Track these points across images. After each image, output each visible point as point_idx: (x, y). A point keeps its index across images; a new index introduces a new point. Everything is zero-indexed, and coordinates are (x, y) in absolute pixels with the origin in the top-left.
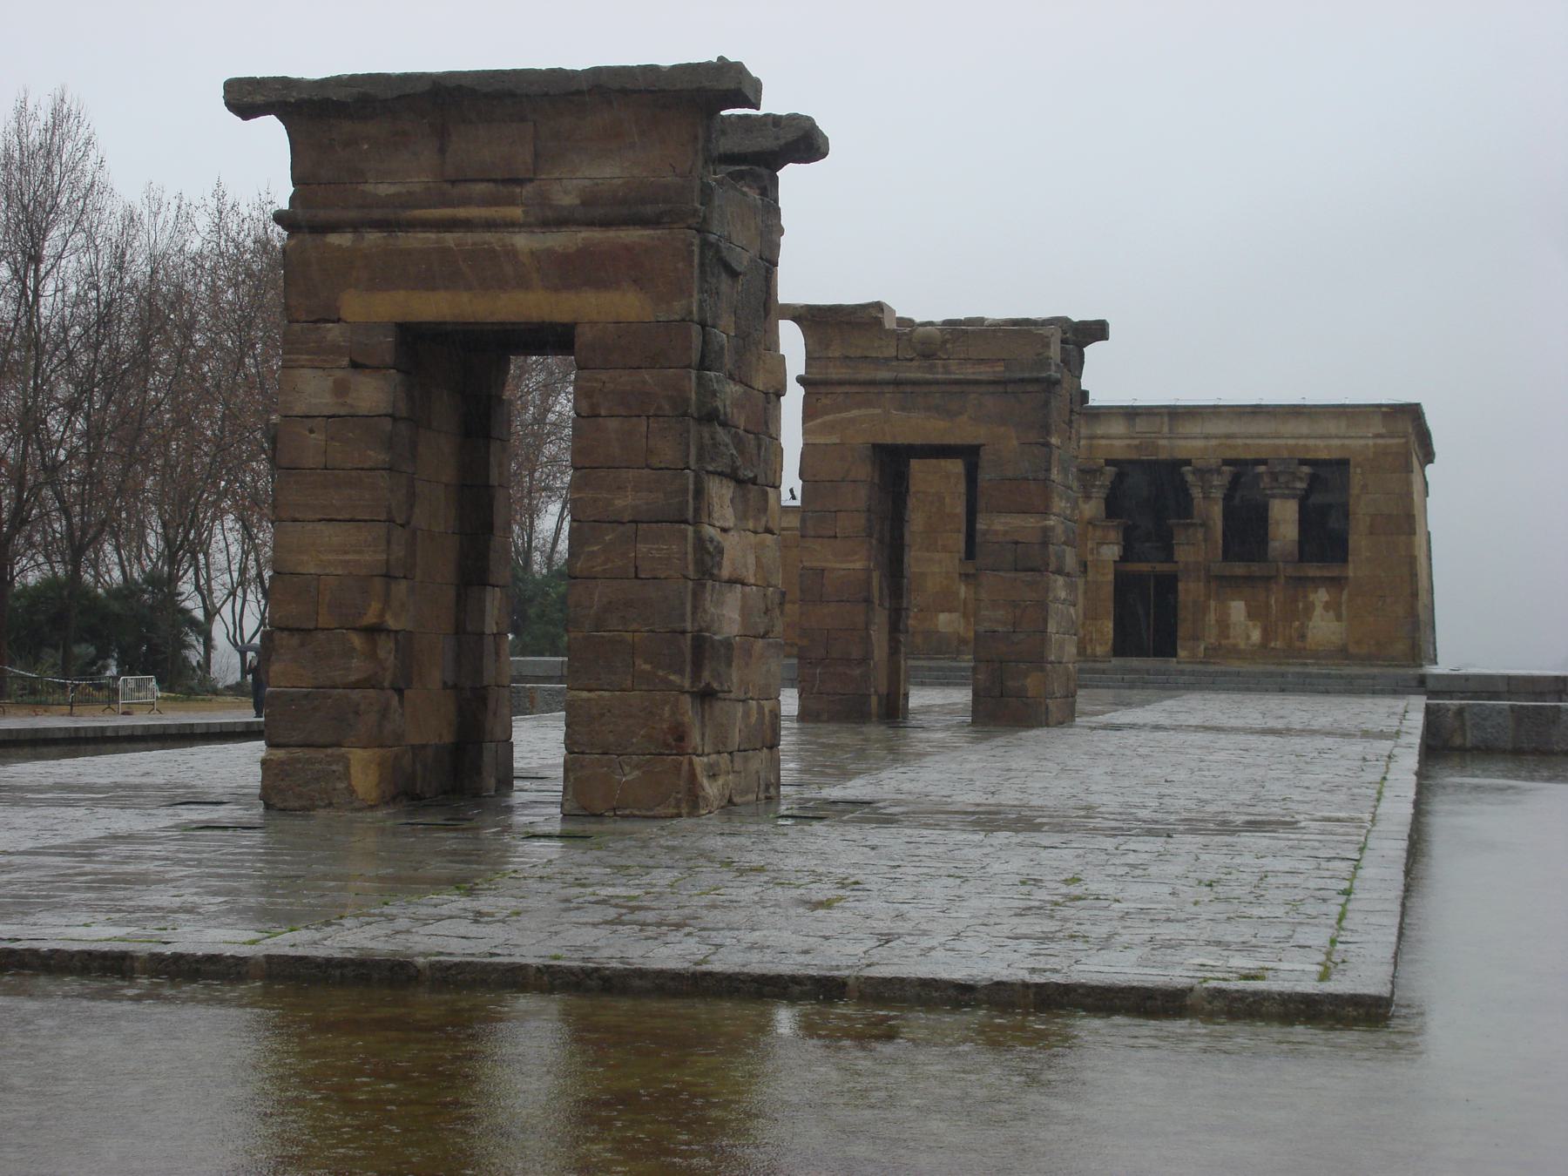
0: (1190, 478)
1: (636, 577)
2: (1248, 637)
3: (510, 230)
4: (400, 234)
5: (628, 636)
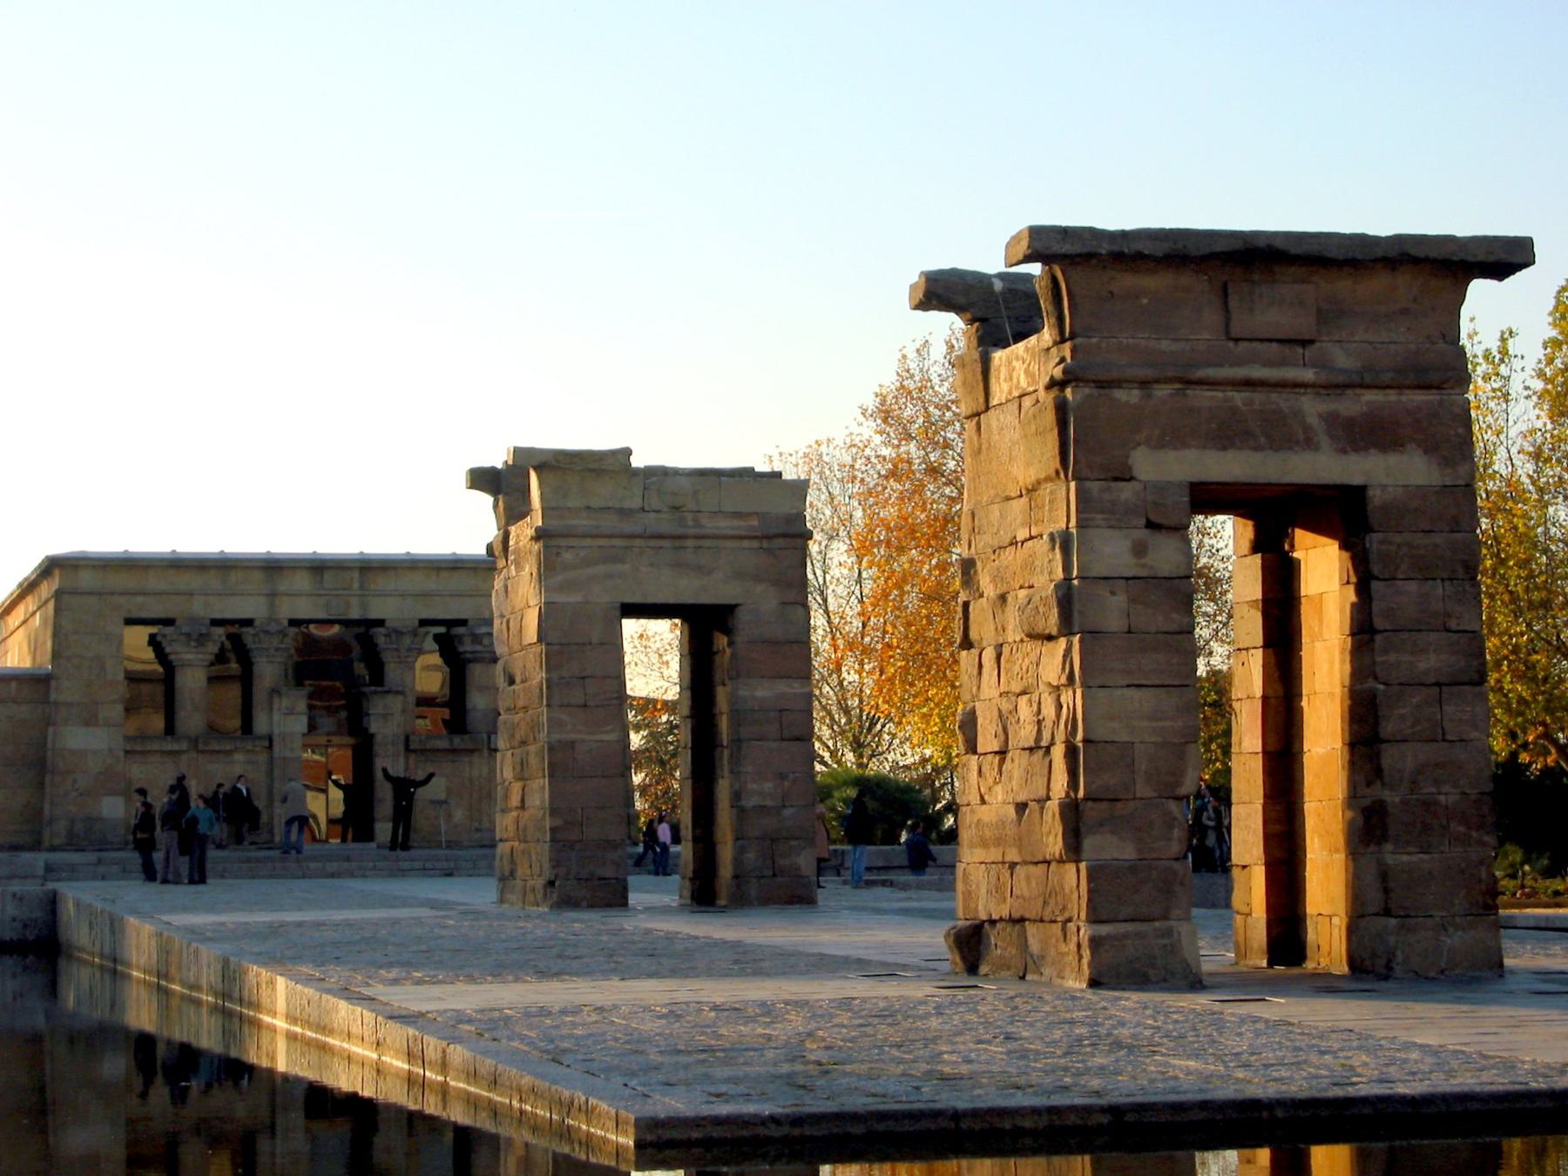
0: (381, 641)
1: (1444, 740)
2: (450, 816)
3: (1297, 390)
4: (1188, 391)
5: (1442, 798)
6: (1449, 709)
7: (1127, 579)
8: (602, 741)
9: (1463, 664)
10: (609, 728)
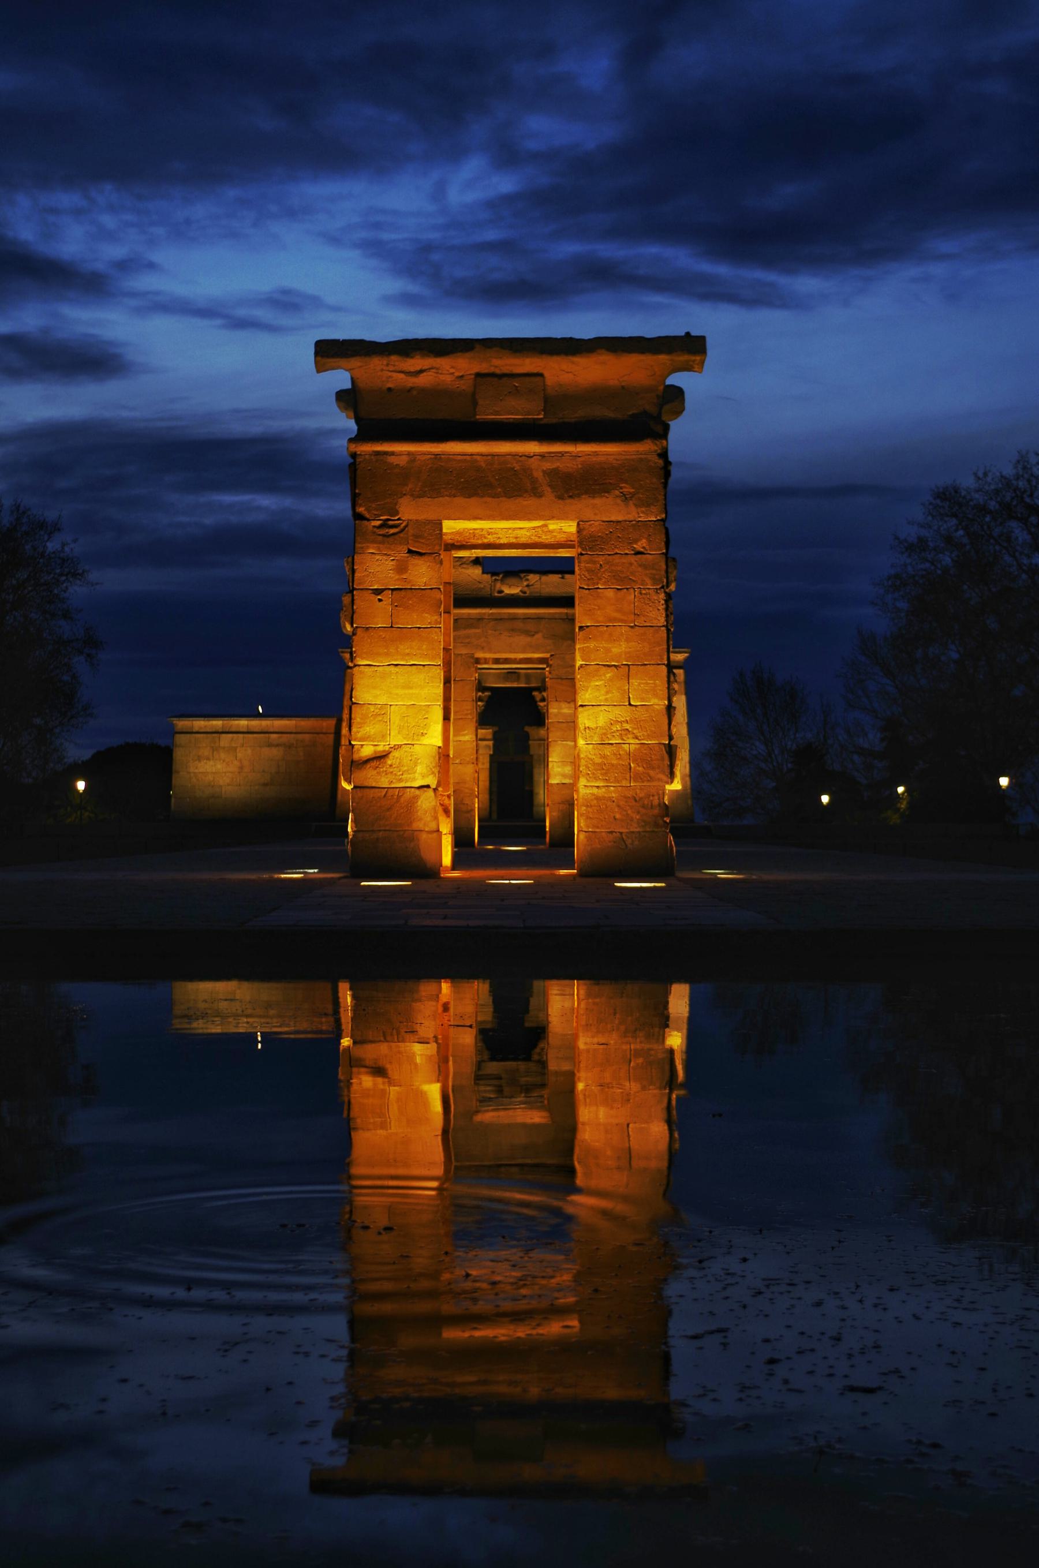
5: (626, 747)
6: (634, 682)
7: (393, 590)
8: (460, 741)
9: (647, 650)
10: (466, 732)
